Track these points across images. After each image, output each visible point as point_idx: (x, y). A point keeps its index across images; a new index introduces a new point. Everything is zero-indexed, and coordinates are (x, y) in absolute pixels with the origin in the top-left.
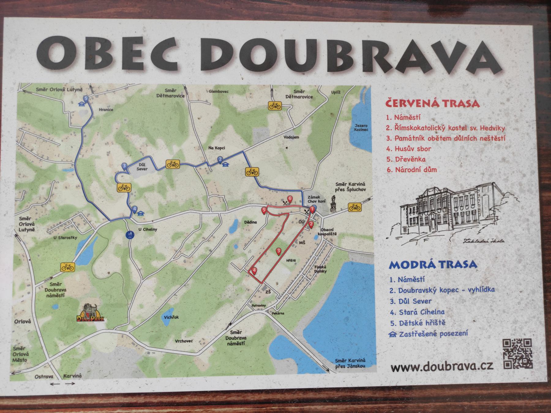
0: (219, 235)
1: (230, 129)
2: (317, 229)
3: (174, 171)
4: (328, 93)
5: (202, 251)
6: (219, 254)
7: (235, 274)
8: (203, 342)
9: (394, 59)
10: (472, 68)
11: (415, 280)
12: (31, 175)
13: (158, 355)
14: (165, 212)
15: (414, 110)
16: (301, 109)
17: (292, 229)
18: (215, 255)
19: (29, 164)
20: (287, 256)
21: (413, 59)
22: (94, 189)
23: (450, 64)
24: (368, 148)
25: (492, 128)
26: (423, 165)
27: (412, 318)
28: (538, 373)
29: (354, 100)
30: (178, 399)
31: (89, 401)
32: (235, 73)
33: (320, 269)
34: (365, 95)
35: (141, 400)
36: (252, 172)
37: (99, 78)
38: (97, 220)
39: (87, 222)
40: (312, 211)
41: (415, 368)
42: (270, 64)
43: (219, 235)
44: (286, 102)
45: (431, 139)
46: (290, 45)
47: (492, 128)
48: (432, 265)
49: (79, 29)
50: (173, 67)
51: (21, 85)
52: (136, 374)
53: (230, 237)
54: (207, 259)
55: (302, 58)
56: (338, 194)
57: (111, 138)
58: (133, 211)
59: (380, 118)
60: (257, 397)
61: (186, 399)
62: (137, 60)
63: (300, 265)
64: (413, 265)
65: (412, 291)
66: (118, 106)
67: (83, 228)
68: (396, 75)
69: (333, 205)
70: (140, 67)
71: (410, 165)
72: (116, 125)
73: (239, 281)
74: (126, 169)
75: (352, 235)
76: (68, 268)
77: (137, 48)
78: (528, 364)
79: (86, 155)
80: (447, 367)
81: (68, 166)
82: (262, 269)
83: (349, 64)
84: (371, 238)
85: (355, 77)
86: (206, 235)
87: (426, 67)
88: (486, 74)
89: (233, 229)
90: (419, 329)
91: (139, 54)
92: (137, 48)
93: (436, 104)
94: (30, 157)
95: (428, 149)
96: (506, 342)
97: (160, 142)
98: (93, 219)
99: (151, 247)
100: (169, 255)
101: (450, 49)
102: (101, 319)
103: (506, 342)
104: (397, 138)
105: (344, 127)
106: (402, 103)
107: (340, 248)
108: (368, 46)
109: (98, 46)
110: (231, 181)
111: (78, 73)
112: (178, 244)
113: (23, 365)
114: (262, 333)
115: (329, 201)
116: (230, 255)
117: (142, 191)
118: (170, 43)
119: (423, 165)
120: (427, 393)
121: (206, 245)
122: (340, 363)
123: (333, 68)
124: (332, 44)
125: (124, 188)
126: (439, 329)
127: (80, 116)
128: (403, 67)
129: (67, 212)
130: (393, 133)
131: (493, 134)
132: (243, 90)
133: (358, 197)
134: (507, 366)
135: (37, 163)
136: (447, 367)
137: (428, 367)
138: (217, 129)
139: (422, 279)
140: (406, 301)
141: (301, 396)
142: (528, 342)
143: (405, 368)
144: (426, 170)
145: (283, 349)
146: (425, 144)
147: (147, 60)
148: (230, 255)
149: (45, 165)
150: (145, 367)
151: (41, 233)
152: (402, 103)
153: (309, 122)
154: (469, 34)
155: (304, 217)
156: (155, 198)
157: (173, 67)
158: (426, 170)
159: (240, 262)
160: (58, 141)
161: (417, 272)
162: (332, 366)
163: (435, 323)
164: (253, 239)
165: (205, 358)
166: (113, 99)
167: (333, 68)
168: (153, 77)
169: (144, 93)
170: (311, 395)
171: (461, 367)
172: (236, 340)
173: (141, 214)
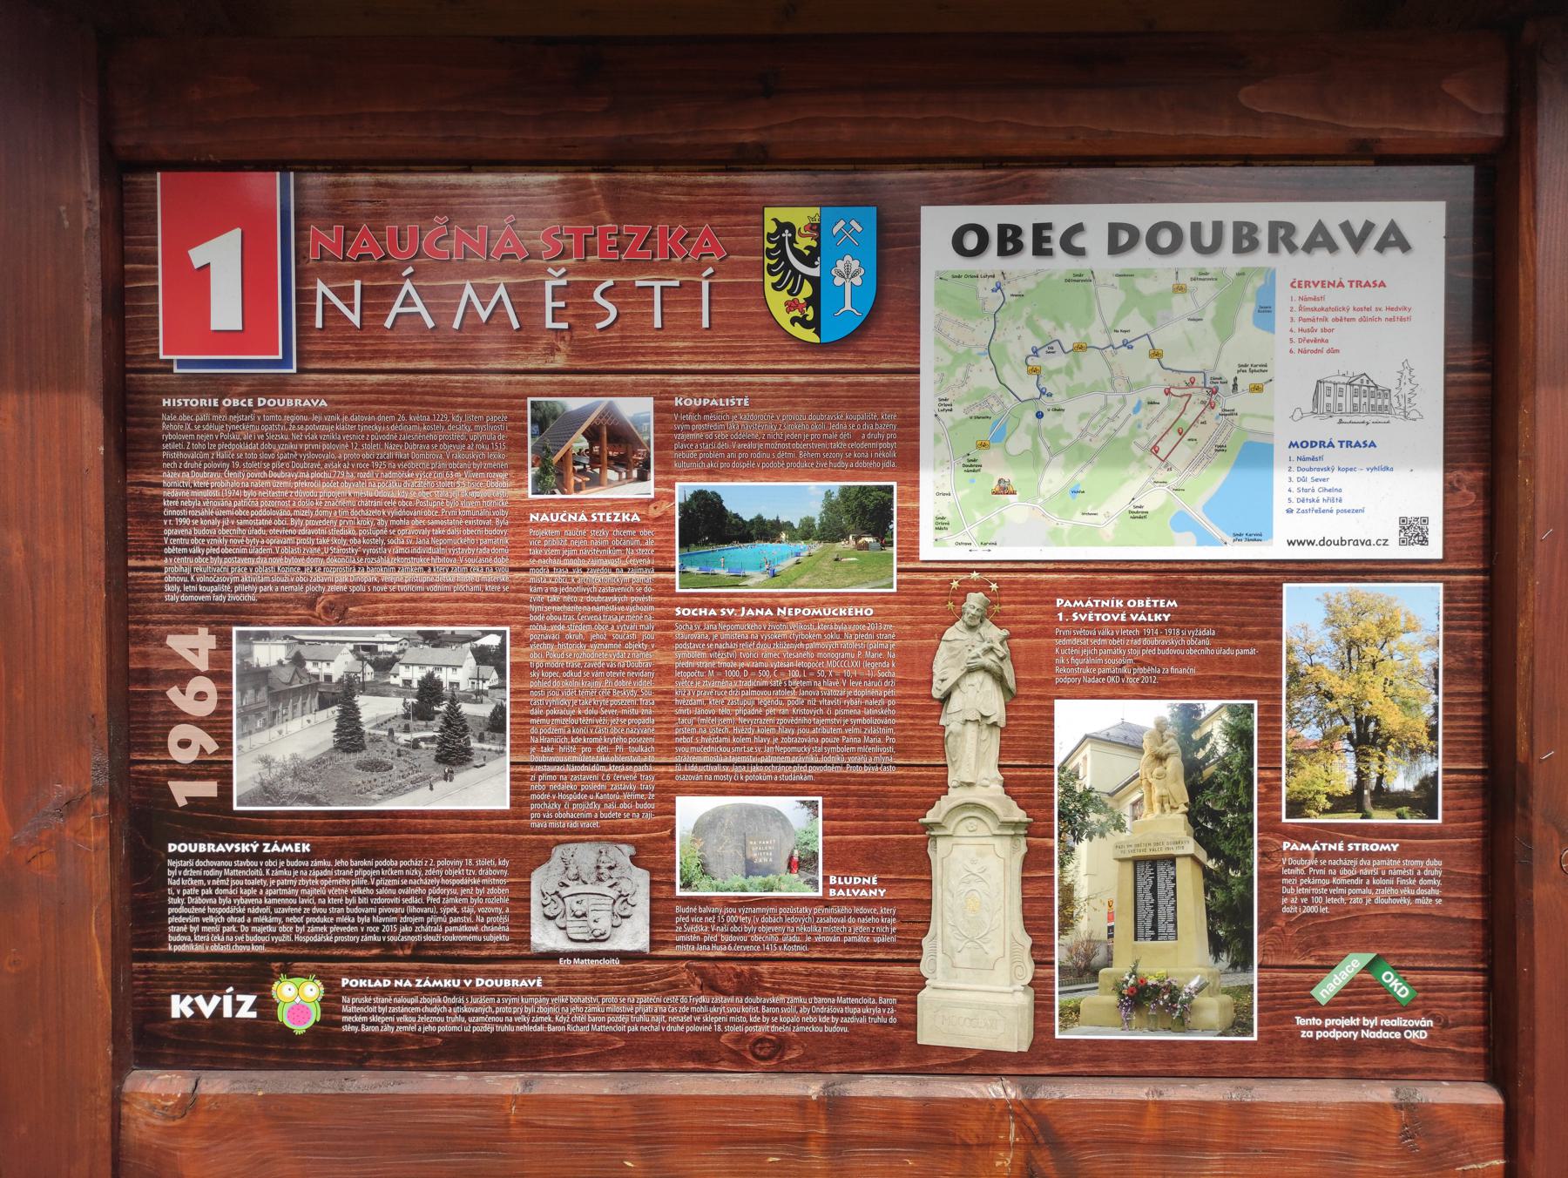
0: (1123, 415)
1: (1136, 310)
2: (1218, 410)
3: (1081, 354)
4: (1233, 275)
5: (1106, 431)
6: (1123, 433)
7: (1139, 452)
8: (1107, 515)
9: (1300, 239)
10: (1380, 247)
11: (1313, 459)
12: (948, 358)
13: (1066, 527)
14: (1072, 394)
15: (1319, 291)
16: (1205, 291)
17: (1194, 410)
18: (1120, 434)
19: (947, 349)
20: (1188, 436)
21: (1320, 239)
22: (1007, 373)
23: (1357, 243)
24: (1271, 329)
25: (1397, 309)
26: (1326, 347)
27: (1309, 495)
28: (1434, 550)
29: (1258, 282)
30: (1085, 567)
31: (1004, 566)
32: (1141, 256)
33: (1221, 448)
34: (1271, 276)
35: (1051, 566)
36: (1156, 354)
37: (1009, 264)
38: (1009, 401)
39: (1000, 402)
40: (1214, 392)
41: (1311, 543)
42: (1175, 247)
43: (1123, 415)
44: (1191, 284)
45: (1336, 320)
46: (1196, 227)
47: (1397, 309)
48: (1331, 444)
49: (991, 216)
50: (1080, 252)
51: (937, 273)
52: (1046, 544)
53: (1134, 417)
54: (1111, 438)
55: (1207, 240)
56: (1239, 376)
57: (1021, 323)
58: (1042, 392)
59: (1284, 299)
60: (1157, 566)
61: (1092, 566)
62: (1046, 246)
63: (1201, 444)
64: (1313, 444)
65: (1311, 469)
66: (1029, 291)
67: (996, 409)
68: (1301, 255)
69: (1235, 386)
70: (1049, 253)
71: (1313, 346)
72: (1027, 310)
73: (1143, 457)
74: (1035, 352)
75: (1254, 416)
76: (983, 445)
77: (1046, 233)
78: (1424, 542)
79: (999, 339)
80: (1342, 542)
81: (982, 350)
82: (1164, 449)
83: (1254, 245)
84: (1272, 418)
85: (1261, 258)
86: (1111, 414)
87: (1333, 247)
88: (1394, 253)
89: (1136, 410)
90: (1317, 506)
91: (1048, 240)
92: (1046, 233)
93: (1341, 285)
94: (946, 341)
95: (1331, 330)
96: (1403, 520)
97: (1067, 325)
98: (1006, 402)
99: (1060, 427)
100: (1075, 436)
101: (1357, 230)
102: (1014, 493)
103: (1403, 520)
104: (1300, 319)
105: (1248, 310)
106: (1307, 284)
107: (1240, 428)
108: (1274, 226)
109: (1010, 233)
110: (1137, 364)
111: (991, 260)
112: (1084, 423)
113: (943, 534)
114: (1161, 510)
115: (1231, 383)
116: (1133, 434)
117: (1050, 373)
118: (1078, 228)
119: (1326, 347)
120: (1322, 567)
121: (1111, 424)
122: (1238, 537)
123: (1238, 249)
124: (1238, 226)
125: (1035, 371)
126: (1336, 506)
127: (994, 301)
128: (1309, 247)
129: (982, 396)
130: (1297, 314)
131: (1399, 314)
132: (1148, 273)
133: (1258, 378)
134: (1402, 542)
135: (953, 347)
136: (1342, 542)
137: (1324, 542)
138: (1123, 311)
139: (1321, 458)
140: (1304, 480)
141: (1199, 566)
142: (1425, 520)
143: (1301, 543)
144: (1329, 351)
145: (1182, 522)
146: (1328, 325)
147: (1055, 245)
148: (1133, 434)
149: (961, 349)
150: (1055, 537)
151: (959, 413)
152: (1307, 284)
153: (1213, 305)
154: (1380, 213)
155: (1205, 398)
156: (1062, 380)
157: (1080, 252)
158: (1329, 351)
159: (1143, 441)
160: (972, 325)
161: (1317, 452)
162: (1229, 539)
163: (1333, 500)
164: (1156, 419)
165: (1109, 529)
166: (1023, 285)
167: (1238, 249)
168: (1061, 262)
169: (1055, 278)
170: (1209, 566)
171: (1356, 543)
172: (1138, 514)
173: (1050, 395)
